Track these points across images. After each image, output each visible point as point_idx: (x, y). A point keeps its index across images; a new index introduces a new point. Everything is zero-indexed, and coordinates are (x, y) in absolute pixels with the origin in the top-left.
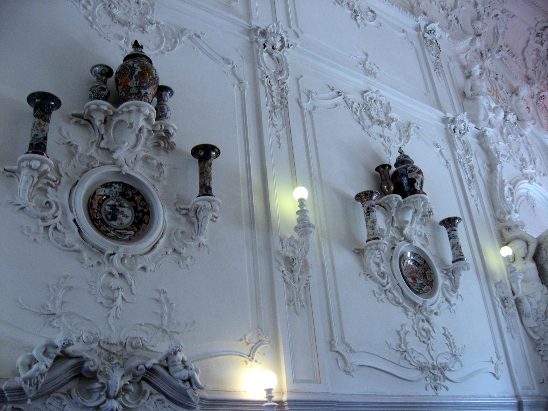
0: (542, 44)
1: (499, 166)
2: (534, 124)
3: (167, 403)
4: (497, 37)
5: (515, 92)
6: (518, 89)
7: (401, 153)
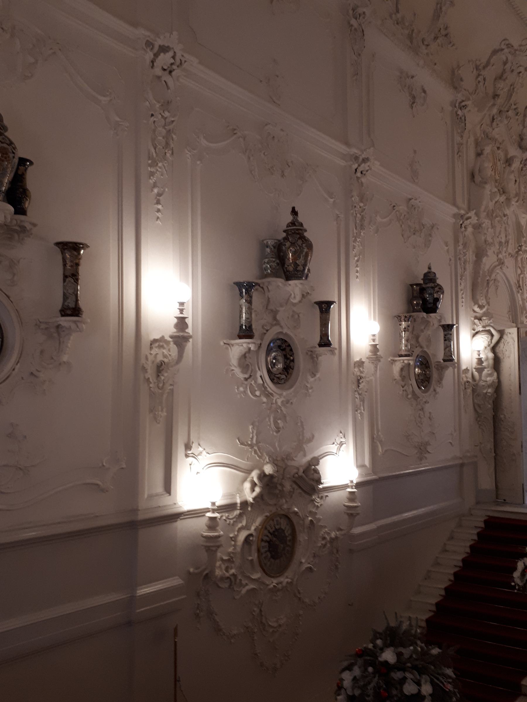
1: (485, 258)
2: (517, 202)
3: (303, 494)
5: (509, 161)
7: (430, 268)
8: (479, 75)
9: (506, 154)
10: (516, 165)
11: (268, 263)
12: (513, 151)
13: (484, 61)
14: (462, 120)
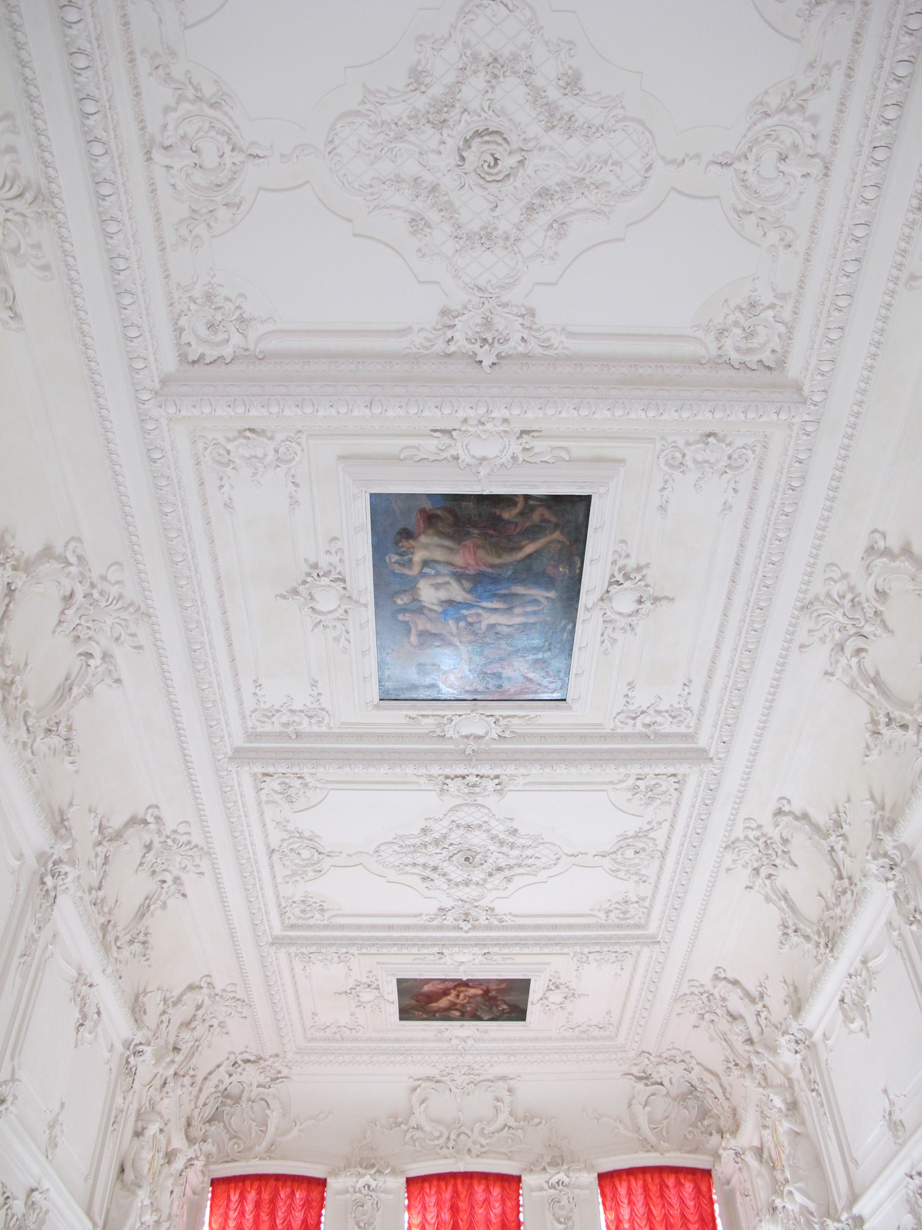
0: (230, 1075)
4: (194, 1054)
5: (170, 1157)
6: (176, 1155)
8: (164, 1012)
9: (169, 1142)
10: (179, 1164)
12: (179, 1142)
13: (176, 993)
14: (131, 1072)
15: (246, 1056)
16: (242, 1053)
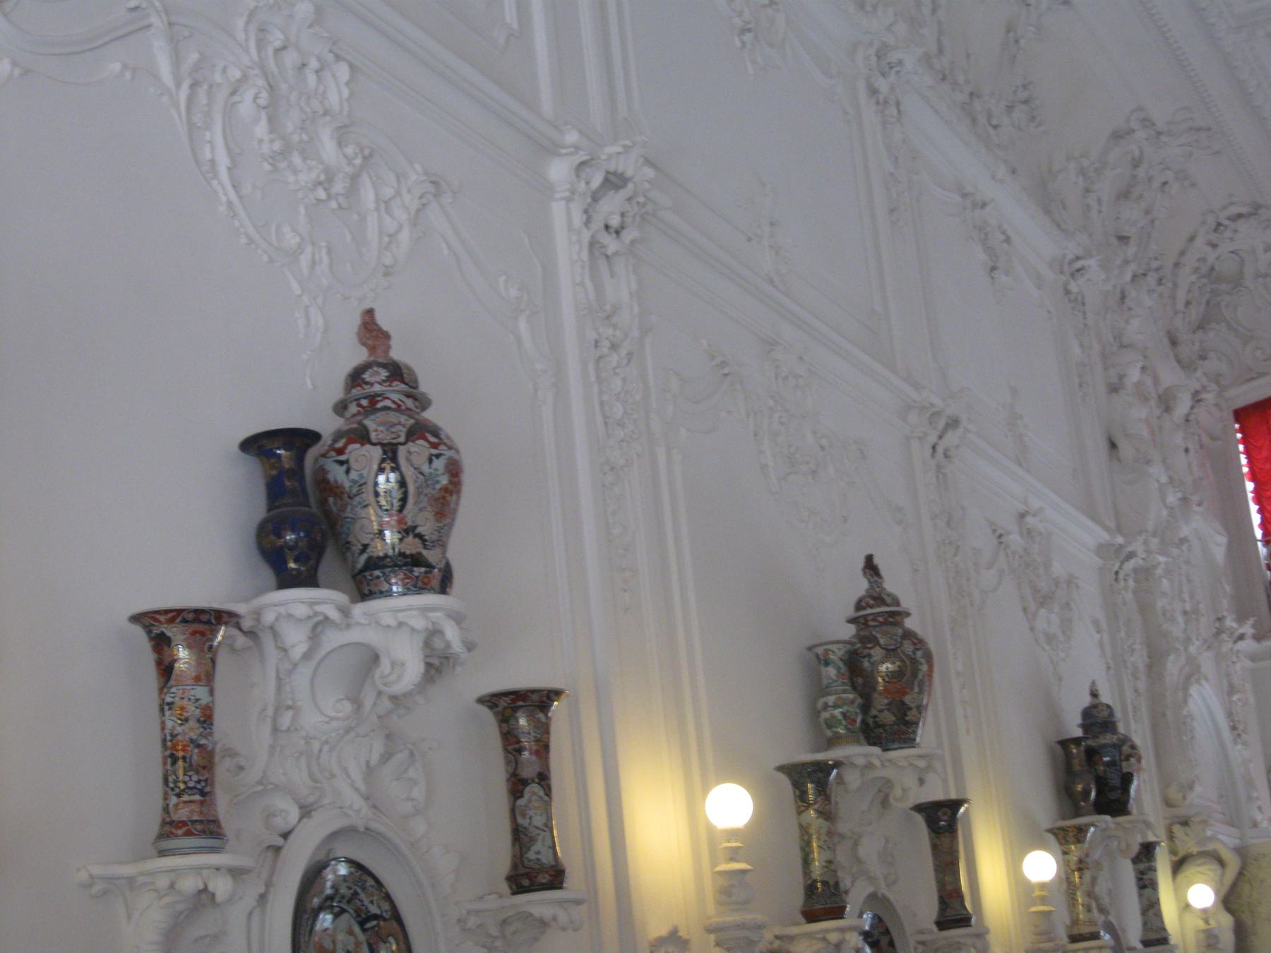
1: (1171, 658)
7: (1094, 695)
8: (1088, 191)
9: (1156, 380)
10: (1183, 405)
11: (835, 706)
12: (1170, 375)
15: (1234, 210)
16: (1225, 208)
